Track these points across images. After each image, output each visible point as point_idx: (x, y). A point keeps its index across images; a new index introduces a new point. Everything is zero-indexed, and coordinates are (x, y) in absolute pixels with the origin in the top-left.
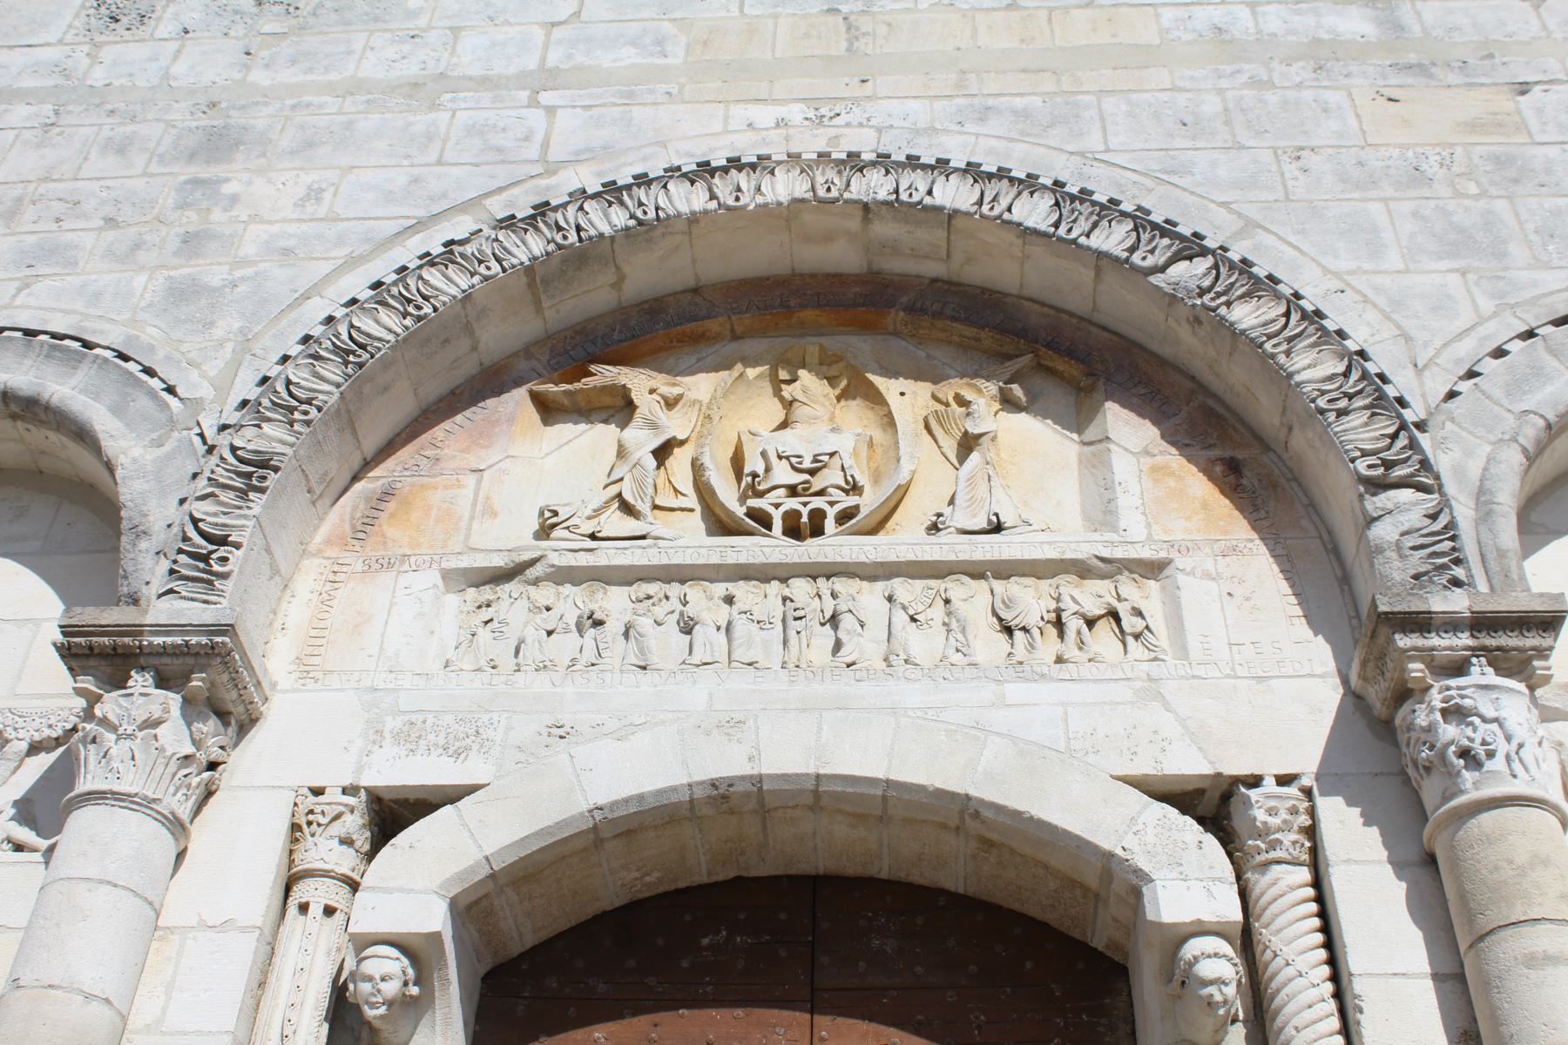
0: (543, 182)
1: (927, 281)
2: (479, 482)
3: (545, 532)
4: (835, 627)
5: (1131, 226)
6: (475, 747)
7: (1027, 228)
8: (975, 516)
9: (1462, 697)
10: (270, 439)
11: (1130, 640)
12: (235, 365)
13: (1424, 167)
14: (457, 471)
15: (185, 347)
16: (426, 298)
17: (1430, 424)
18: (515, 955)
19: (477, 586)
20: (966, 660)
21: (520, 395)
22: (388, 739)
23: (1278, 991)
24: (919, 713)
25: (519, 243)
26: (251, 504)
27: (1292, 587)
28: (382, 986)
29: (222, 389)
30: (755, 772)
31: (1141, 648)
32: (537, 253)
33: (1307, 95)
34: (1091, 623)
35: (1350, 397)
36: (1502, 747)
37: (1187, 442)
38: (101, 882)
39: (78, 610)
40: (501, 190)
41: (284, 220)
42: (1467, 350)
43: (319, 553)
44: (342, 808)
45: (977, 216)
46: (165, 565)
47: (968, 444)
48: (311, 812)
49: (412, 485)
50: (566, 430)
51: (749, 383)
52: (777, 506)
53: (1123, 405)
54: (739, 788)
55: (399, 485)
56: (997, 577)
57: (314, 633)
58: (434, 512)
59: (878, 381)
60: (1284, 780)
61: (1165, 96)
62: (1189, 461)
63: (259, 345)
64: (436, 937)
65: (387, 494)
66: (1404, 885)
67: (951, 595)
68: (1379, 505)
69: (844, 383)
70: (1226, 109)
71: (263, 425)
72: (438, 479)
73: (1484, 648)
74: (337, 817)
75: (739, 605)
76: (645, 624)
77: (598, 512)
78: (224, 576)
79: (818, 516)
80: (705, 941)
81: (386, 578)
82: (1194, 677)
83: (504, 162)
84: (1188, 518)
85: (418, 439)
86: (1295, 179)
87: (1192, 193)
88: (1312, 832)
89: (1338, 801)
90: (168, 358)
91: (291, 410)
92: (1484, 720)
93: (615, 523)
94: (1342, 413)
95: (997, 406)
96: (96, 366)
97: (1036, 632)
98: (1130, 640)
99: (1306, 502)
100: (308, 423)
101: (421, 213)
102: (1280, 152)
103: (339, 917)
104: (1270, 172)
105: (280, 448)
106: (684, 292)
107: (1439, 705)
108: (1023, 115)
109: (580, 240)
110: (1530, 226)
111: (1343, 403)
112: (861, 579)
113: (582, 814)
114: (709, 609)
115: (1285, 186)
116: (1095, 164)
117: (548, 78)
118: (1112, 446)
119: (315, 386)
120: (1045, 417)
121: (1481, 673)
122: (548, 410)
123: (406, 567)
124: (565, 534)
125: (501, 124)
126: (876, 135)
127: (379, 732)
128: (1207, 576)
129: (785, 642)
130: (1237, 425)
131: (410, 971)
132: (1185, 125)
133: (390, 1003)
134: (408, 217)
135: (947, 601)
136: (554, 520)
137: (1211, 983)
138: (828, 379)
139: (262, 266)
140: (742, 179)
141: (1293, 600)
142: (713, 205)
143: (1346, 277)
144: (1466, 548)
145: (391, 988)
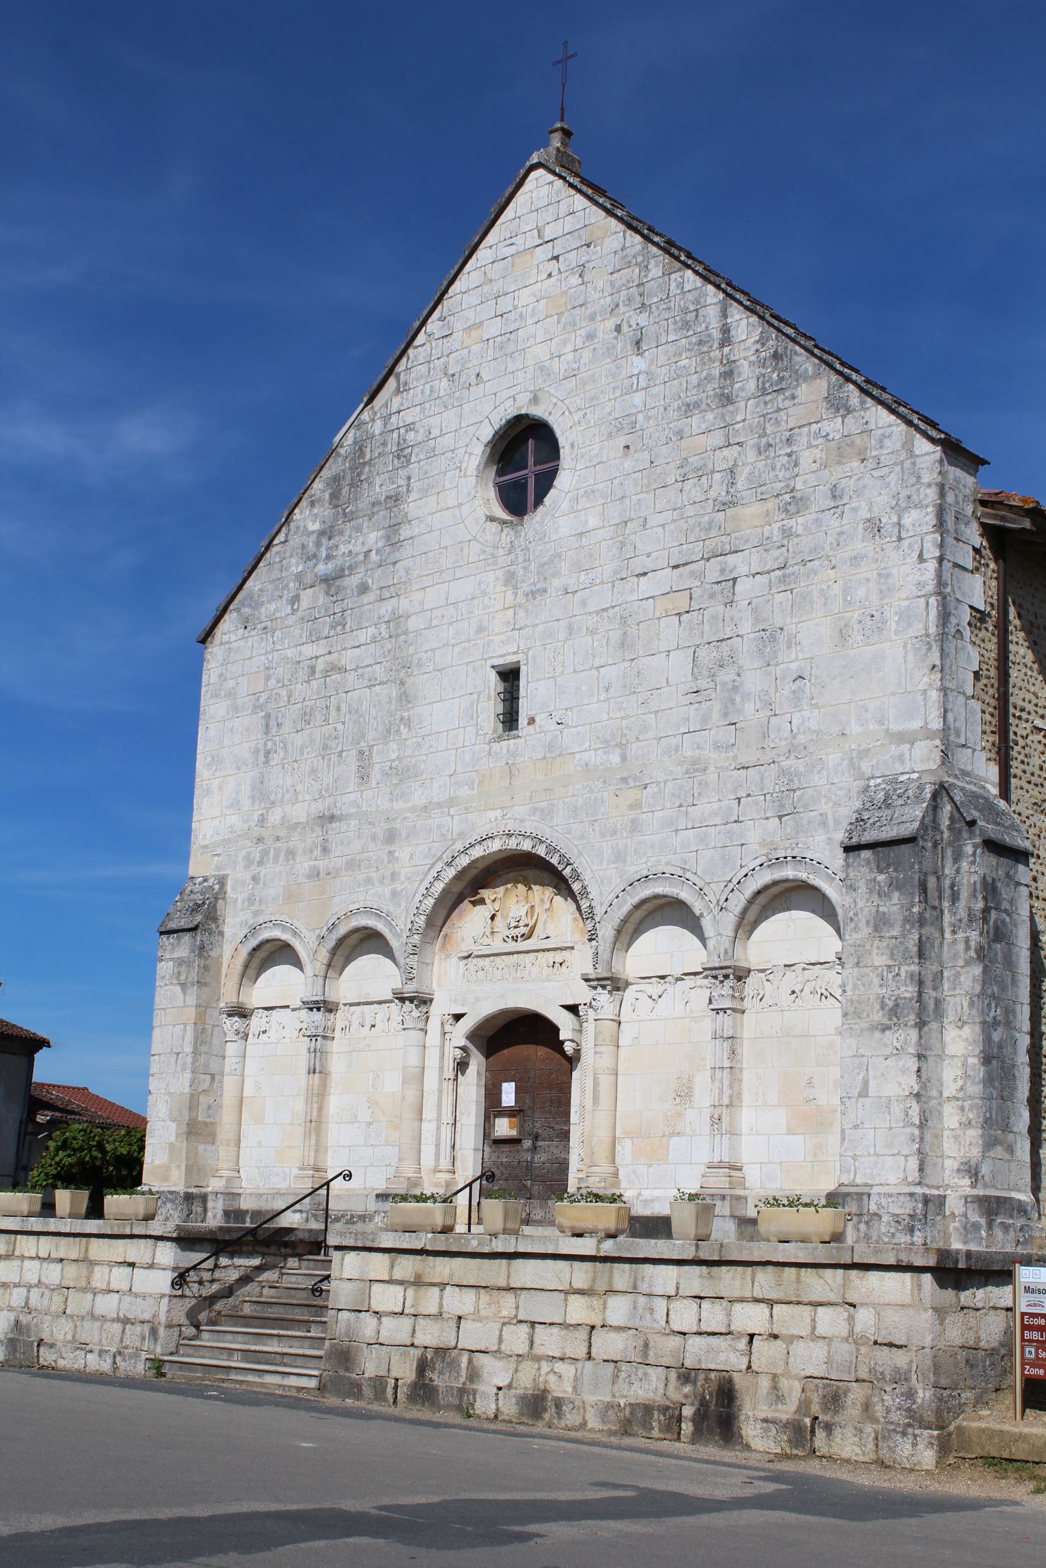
21: (466, 901)
29: (405, 925)
42: (612, 896)
61: (570, 799)
65: (446, 936)
108: (542, 810)
117: (451, 802)
121: (600, 990)
122: (474, 903)
140: (489, 842)
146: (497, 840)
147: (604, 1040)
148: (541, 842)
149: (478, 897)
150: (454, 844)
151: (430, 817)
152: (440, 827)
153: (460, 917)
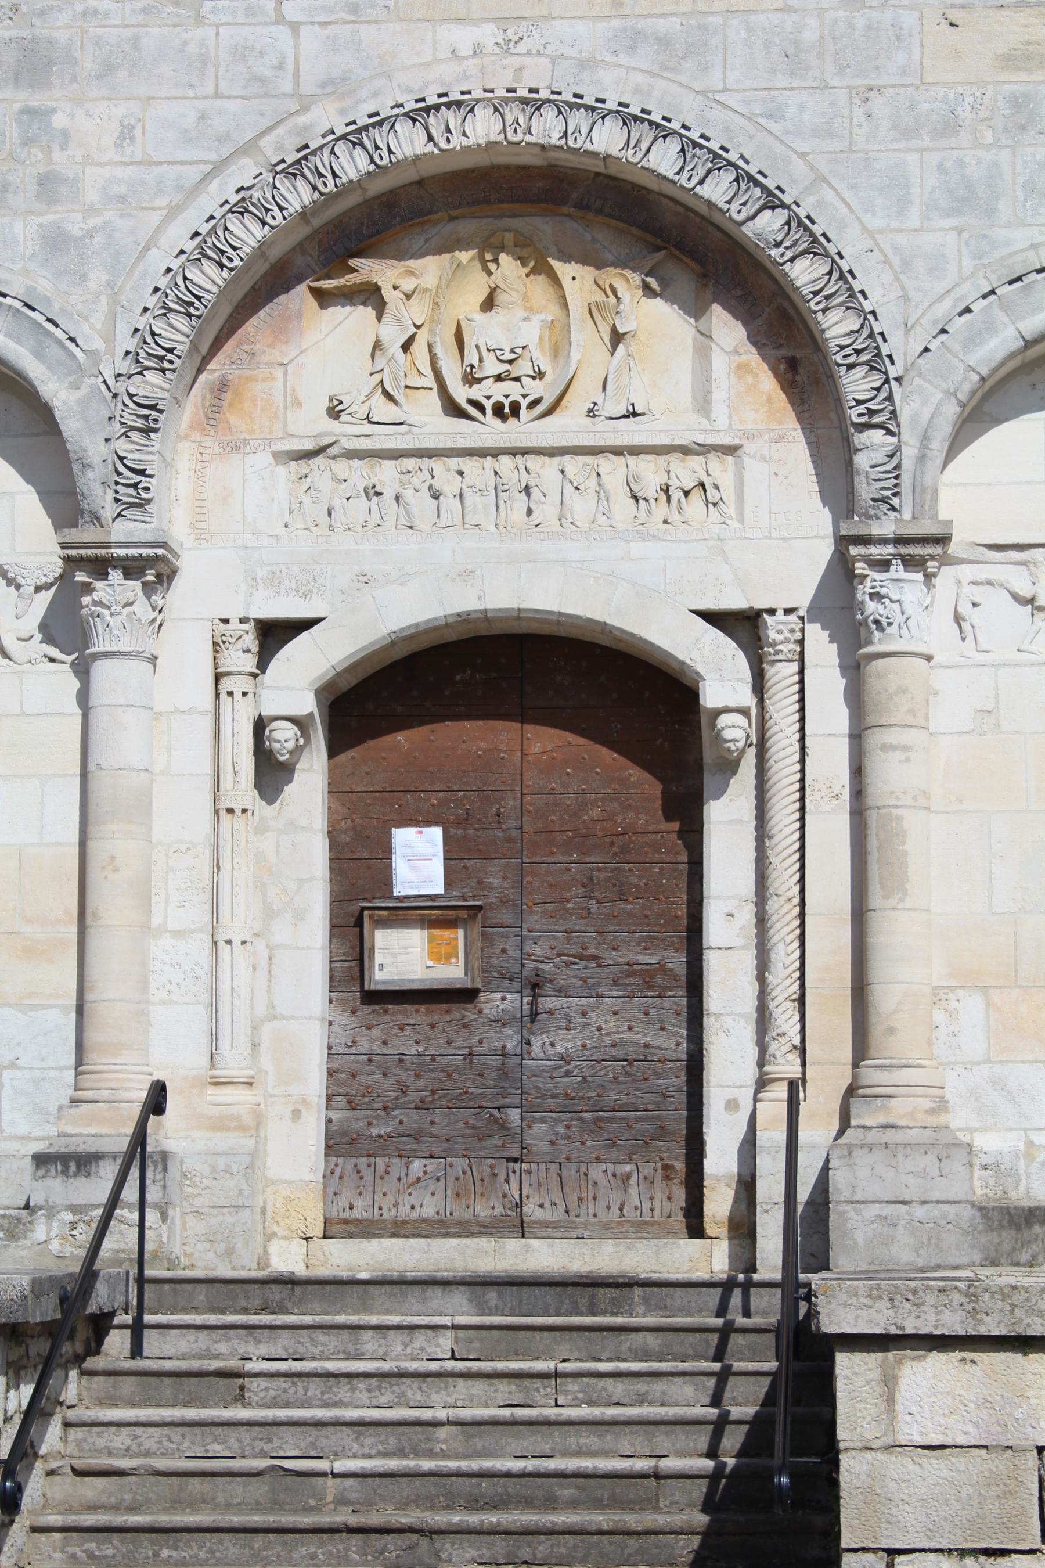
0: (302, 120)
1: (592, 176)
2: (286, 374)
3: (334, 413)
4: (528, 494)
5: (733, 177)
6: (315, 591)
7: (659, 174)
8: (619, 403)
9: (881, 587)
10: (153, 385)
11: (710, 506)
12: (112, 318)
13: (959, 111)
14: (270, 364)
15: (72, 299)
16: (235, 249)
17: (905, 379)
18: (346, 689)
19: (296, 460)
20: (609, 522)
21: (302, 289)
22: (261, 586)
23: (770, 738)
24: (580, 566)
25: (293, 190)
26: (153, 443)
27: (815, 468)
28: (286, 745)
29: (109, 339)
30: (482, 608)
31: (717, 513)
32: (307, 202)
33: (888, 16)
34: (687, 493)
35: (858, 352)
36: (898, 619)
37: (764, 342)
38: (127, 706)
39: (66, 531)
40: (270, 129)
41: (111, 163)
42: (946, 308)
43: (186, 437)
44: (242, 633)
45: (624, 160)
46: (111, 495)
47: (617, 338)
48: (224, 635)
49: (240, 378)
50: (337, 312)
51: (464, 267)
52: (488, 398)
53: (724, 308)
54: (473, 616)
55: (230, 377)
56: (631, 454)
57: (197, 503)
58: (259, 402)
59: (554, 263)
60: (788, 611)
61: (775, 18)
62: (764, 360)
63: (123, 297)
64: (311, 714)
65: (223, 386)
66: (844, 681)
67: (601, 471)
68: (862, 441)
69: (532, 264)
70: (822, 37)
71: (145, 372)
72: (255, 372)
73: (900, 555)
74: (240, 637)
75: (467, 480)
76: (408, 494)
77: (368, 397)
78: (149, 501)
79: (515, 409)
80: (458, 678)
81: (237, 457)
82: (745, 538)
83: (266, 95)
84: (757, 411)
85: (236, 335)
86: (860, 126)
87: (782, 142)
88: (801, 642)
89: (818, 625)
90: (63, 310)
91: (161, 358)
92: (892, 601)
93: (382, 410)
94: (851, 367)
95: (640, 292)
96: (10, 314)
97: (652, 502)
98: (710, 506)
99: (836, 397)
100: (174, 370)
101: (213, 157)
102: (854, 92)
103: (250, 696)
104: (843, 117)
105: (161, 394)
106: (411, 184)
107: (868, 590)
108: (664, 42)
109: (336, 186)
110: (1020, 180)
111: (851, 360)
112: (544, 455)
113: (384, 637)
114: (448, 481)
115: (851, 134)
116: (714, 105)
118: (713, 345)
119: (173, 337)
120: (673, 304)
121: (897, 570)
122: (323, 298)
123: (248, 450)
124: (349, 418)
125: (258, 46)
126: (550, 65)
127: (254, 579)
128: (763, 458)
129: (497, 507)
130: (801, 327)
131: (299, 733)
132: (787, 56)
133: (291, 753)
134: (205, 162)
135: (598, 475)
136: (340, 408)
137: (730, 741)
138: (519, 258)
139: (108, 215)
140: (452, 117)
141: (814, 479)
142: (430, 148)
143: (877, 236)
144: (903, 485)
145: (290, 745)
146: (483, 115)
147: (912, 712)
148: (662, 131)
149: (350, 279)
150: (304, 109)
151: (200, 20)
152: (241, 53)
153: (281, 332)
